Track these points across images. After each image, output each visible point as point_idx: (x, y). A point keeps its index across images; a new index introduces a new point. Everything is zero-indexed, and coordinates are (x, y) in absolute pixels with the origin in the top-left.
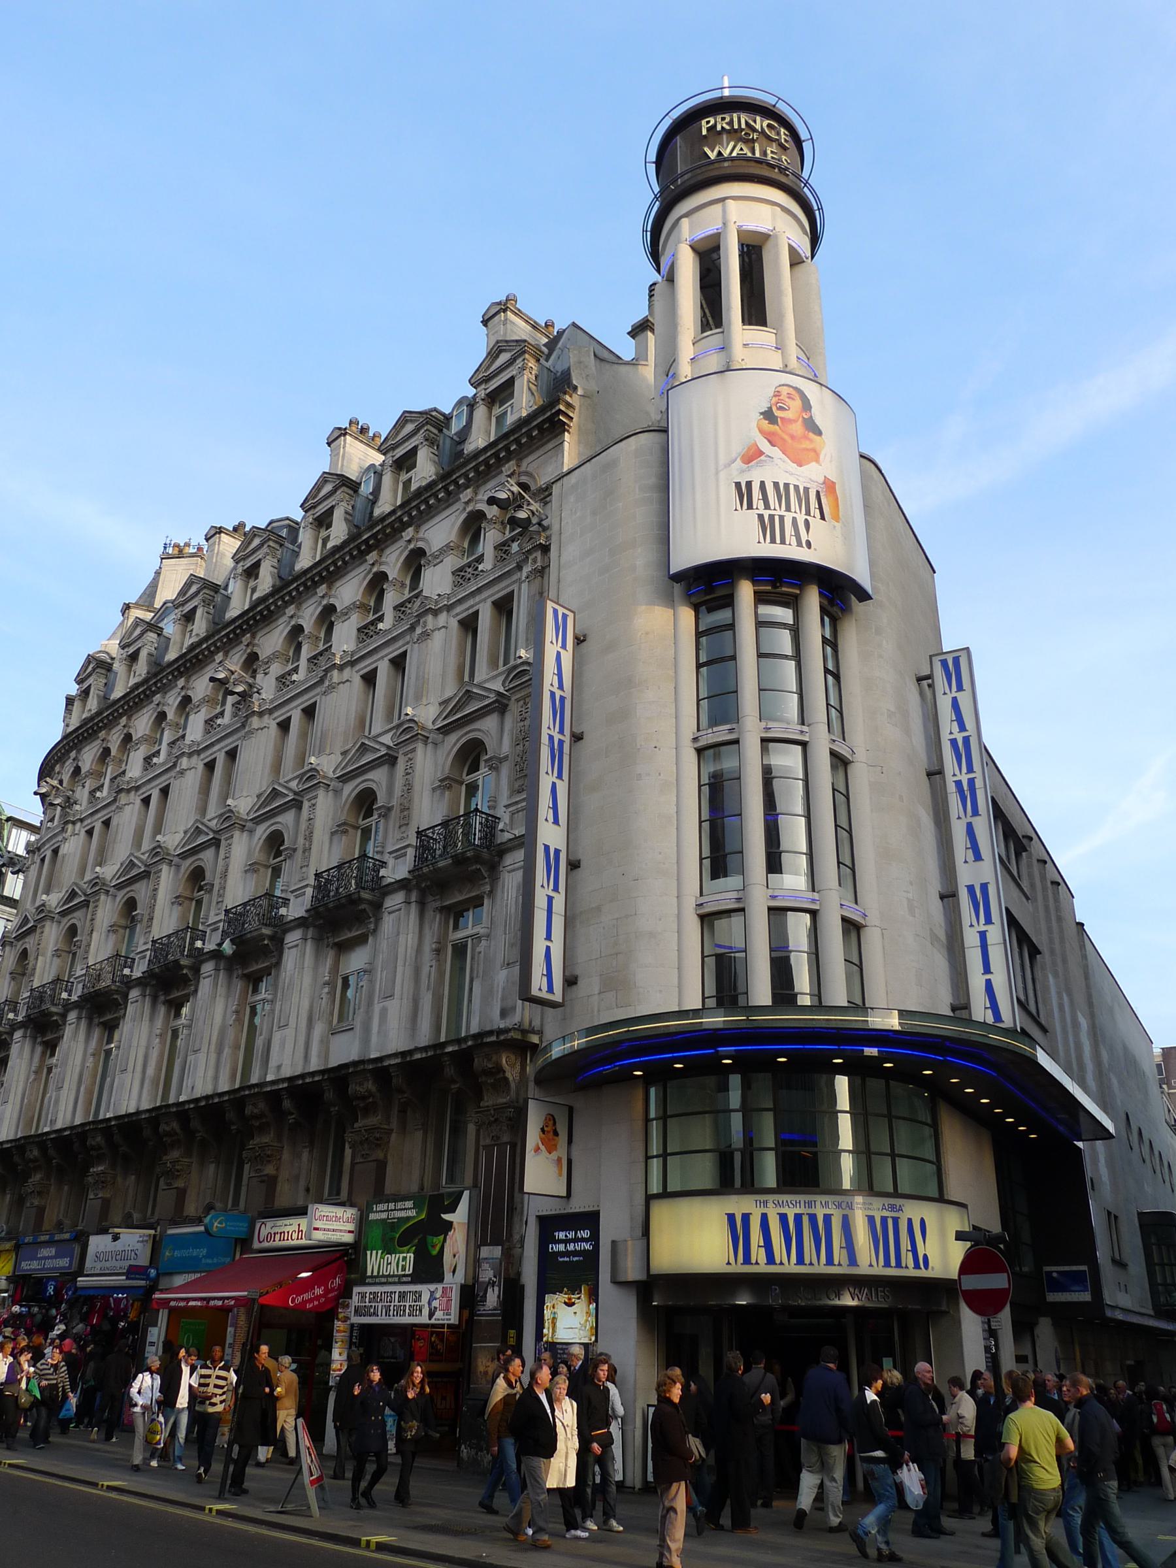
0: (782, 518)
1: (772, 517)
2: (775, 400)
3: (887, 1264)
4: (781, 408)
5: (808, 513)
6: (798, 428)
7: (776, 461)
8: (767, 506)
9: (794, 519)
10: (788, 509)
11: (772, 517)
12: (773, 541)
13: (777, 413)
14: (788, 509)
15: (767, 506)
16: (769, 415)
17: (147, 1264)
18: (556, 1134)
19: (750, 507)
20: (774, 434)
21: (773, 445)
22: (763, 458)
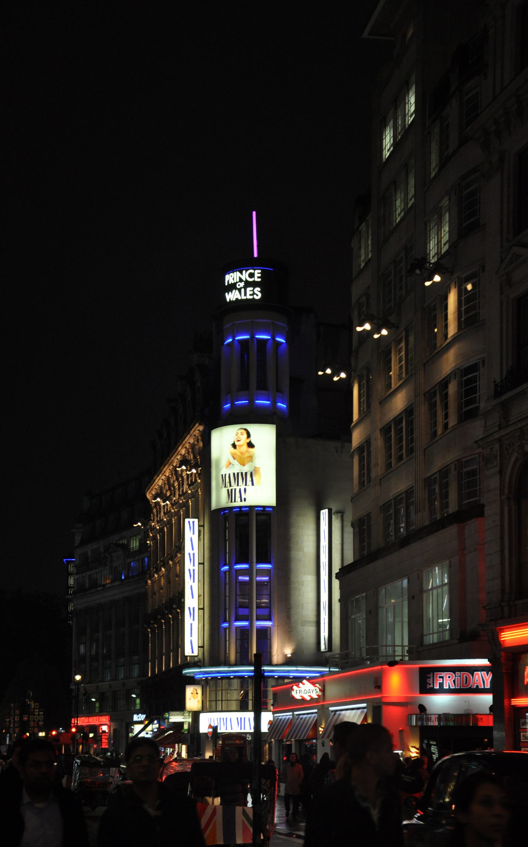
0: (235, 489)
1: (232, 490)
2: (236, 437)
3: (241, 729)
4: (239, 441)
5: (246, 485)
6: (245, 447)
7: (235, 466)
8: (230, 486)
9: (240, 489)
10: (238, 485)
11: (232, 490)
12: (231, 502)
13: (237, 443)
14: (238, 485)
15: (230, 486)
16: (234, 446)
17: (202, 715)
18: (197, 693)
19: (225, 487)
20: (235, 454)
21: (234, 459)
22: (231, 465)
